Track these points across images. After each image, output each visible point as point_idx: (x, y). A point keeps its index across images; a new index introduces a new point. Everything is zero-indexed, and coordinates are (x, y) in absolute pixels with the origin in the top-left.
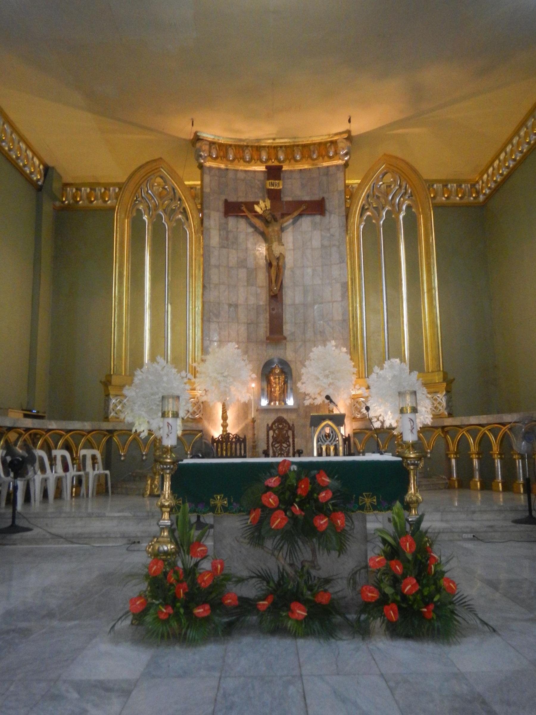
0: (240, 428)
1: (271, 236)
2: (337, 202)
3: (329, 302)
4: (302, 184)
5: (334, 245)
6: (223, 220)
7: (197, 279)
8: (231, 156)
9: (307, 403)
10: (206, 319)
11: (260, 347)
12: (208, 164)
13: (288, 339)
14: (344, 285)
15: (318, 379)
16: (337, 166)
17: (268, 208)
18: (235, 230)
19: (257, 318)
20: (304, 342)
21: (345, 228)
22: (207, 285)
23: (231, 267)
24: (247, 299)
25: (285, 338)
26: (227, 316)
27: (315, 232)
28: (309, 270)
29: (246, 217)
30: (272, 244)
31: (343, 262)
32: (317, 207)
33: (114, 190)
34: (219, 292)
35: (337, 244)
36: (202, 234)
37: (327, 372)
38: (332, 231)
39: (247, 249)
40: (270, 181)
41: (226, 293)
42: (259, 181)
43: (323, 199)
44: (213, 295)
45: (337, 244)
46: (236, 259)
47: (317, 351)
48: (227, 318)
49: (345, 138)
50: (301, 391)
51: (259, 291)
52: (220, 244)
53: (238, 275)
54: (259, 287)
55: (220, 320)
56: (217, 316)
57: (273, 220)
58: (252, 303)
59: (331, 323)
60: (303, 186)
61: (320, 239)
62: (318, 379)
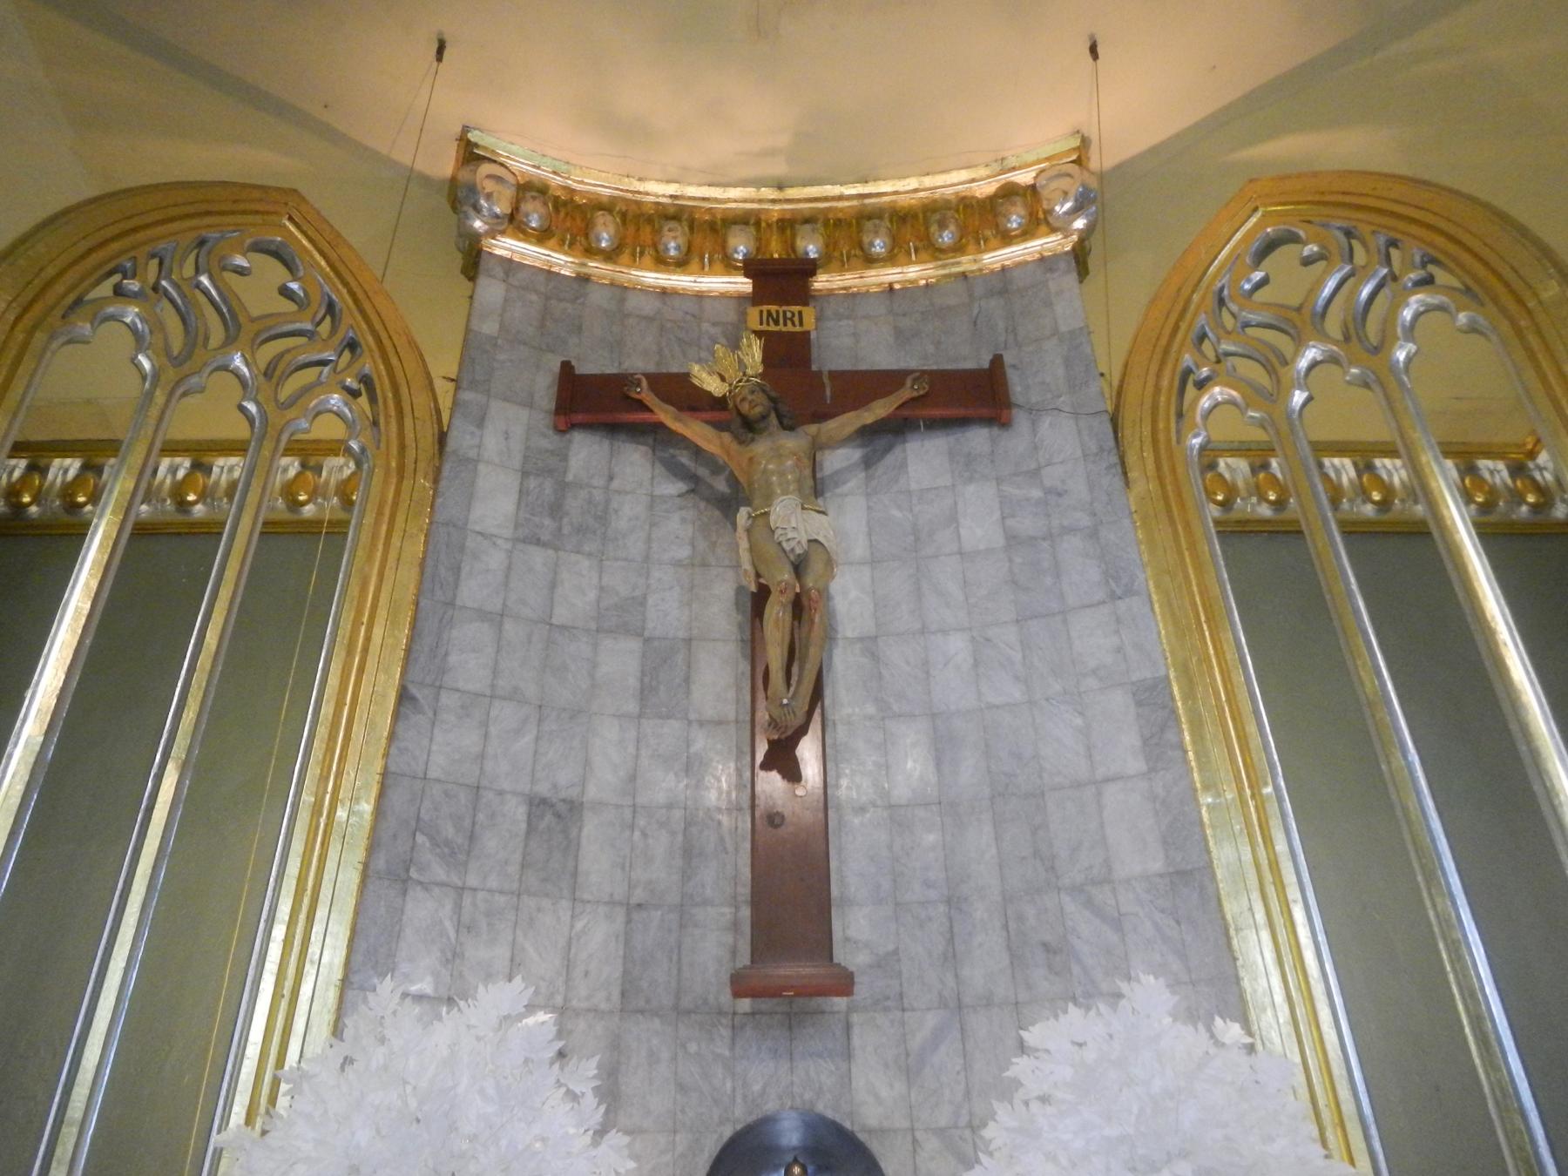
1: (765, 471)
2: (1061, 371)
3: (1078, 785)
4: (898, 332)
6: (549, 441)
10: (389, 871)
11: (693, 1047)
12: (506, 246)
13: (862, 990)
14: (1151, 696)
16: (1045, 263)
17: (749, 371)
18: (599, 482)
19: (686, 875)
20: (957, 1007)
21: (1114, 459)
23: (563, 628)
24: (633, 778)
25: (844, 984)
26: (518, 857)
27: (971, 488)
28: (957, 645)
29: (654, 434)
30: (769, 498)
31: (1129, 592)
32: (973, 397)
33: (173, 470)
35: (1085, 521)
36: (436, 481)
38: (1052, 476)
40: (765, 308)
41: (527, 739)
42: (714, 324)
43: (997, 361)
44: (446, 746)
45: (1085, 521)
46: (592, 595)
47: (1061, 1041)
48: (513, 869)
51: (700, 741)
52: (516, 527)
53: (595, 665)
54: (701, 724)
55: (472, 880)
56: (460, 853)
57: (773, 419)
58: (661, 798)
61: (997, 515)
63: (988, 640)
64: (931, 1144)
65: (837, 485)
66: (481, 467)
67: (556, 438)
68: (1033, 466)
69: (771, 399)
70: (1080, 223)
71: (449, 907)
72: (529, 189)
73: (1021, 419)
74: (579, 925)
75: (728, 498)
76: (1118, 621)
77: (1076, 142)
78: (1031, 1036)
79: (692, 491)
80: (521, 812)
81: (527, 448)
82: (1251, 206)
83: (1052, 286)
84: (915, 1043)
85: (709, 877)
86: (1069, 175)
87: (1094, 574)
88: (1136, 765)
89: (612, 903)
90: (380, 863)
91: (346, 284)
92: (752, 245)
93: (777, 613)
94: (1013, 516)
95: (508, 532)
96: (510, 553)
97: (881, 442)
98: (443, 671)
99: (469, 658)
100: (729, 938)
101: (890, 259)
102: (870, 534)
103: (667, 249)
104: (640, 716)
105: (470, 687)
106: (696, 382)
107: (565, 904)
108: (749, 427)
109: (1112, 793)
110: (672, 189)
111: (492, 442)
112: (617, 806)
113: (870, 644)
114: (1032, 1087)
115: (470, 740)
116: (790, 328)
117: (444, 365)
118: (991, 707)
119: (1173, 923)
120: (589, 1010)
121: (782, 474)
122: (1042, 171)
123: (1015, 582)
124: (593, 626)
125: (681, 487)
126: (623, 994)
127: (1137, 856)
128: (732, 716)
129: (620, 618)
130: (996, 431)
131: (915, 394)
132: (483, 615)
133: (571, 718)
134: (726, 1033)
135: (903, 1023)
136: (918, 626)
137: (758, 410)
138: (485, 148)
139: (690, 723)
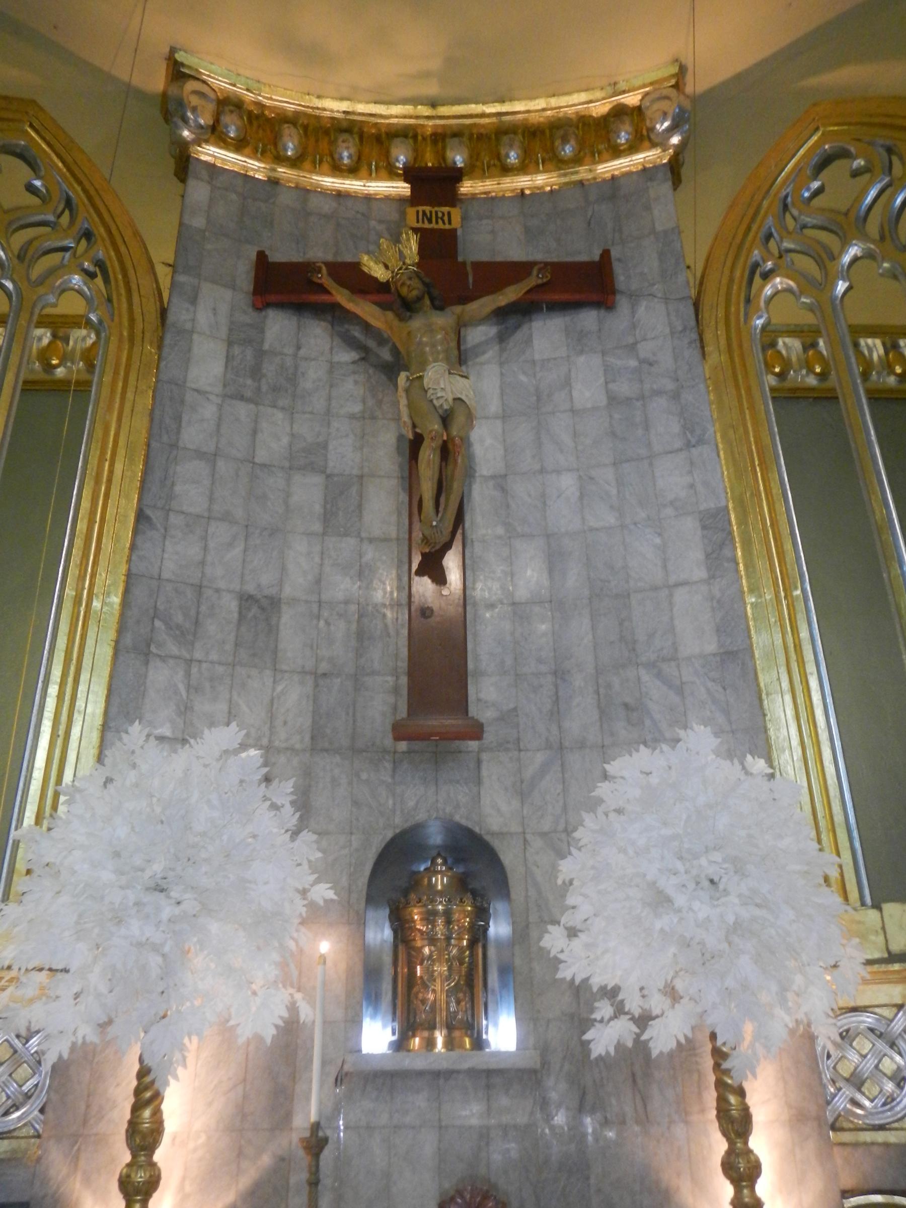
0: (245, 1182)
1: (420, 343)
2: (656, 264)
3: (655, 588)
4: (527, 230)
5: (658, 393)
6: (248, 317)
7: (114, 492)
8: (291, 145)
9: (606, 1038)
10: (135, 645)
11: (364, 776)
12: (210, 153)
13: (490, 736)
14: (714, 523)
15: (660, 900)
16: (647, 172)
17: (408, 261)
18: (289, 350)
19: (359, 652)
20: (560, 749)
21: (694, 336)
22: (155, 515)
23: (264, 466)
24: (318, 581)
25: (476, 731)
26: (232, 637)
27: (582, 359)
28: (568, 482)
29: (333, 313)
30: (423, 366)
31: (701, 441)
32: (585, 285)
34: (205, 548)
36: (160, 347)
37: (708, 865)
38: (645, 350)
39: (328, 412)
40: (421, 208)
41: (237, 551)
42: (380, 222)
43: (606, 254)
44: (175, 555)
45: (670, 386)
46: (285, 440)
47: (632, 771)
48: (229, 647)
49: (672, 86)
50: (565, 973)
51: (370, 553)
52: (225, 386)
53: (288, 495)
54: (371, 540)
55: (198, 655)
56: (189, 633)
57: (427, 302)
58: (340, 596)
59: (669, 669)
60: (531, 235)
61: (602, 380)
62: (660, 900)
63: (591, 478)
64: (537, 843)
65: (477, 356)
66: (195, 337)
67: (255, 314)
68: (631, 340)
69: (424, 283)
70: (675, 140)
71: (181, 673)
72: (228, 104)
73: (623, 303)
74: (279, 688)
75: (391, 365)
76: (692, 463)
77: (674, 70)
78: (611, 768)
79: (363, 359)
80: (234, 605)
81: (232, 323)
82: (812, 126)
83: (652, 193)
84: (528, 773)
85: (375, 655)
86: (667, 98)
87: (676, 428)
88: (701, 573)
89: (303, 672)
90: (128, 640)
91: (80, 183)
92: (410, 155)
93: (428, 455)
94: (614, 381)
95: (218, 389)
96: (220, 407)
97: (512, 321)
98: (171, 497)
99: (191, 489)
100: (391, 699)
101: (522, 169)
102: (502, 394)
103: (341, 158)
104: (324, 534)
105: (192, 510)
106: (366, 269)
107: (268, 672)
108: (407, 308)
109: (680, 595)
110: (344, 106)
111: (203, 317)
112: (306, 602)
113: (500, 481)
114: (611, 802)
115: (194, 551)
116: (441, 225)
117: (163, 252)
118: (591, 529)
119: (721, 690)
120: (287, 749)
121: (433, 346)
122: (646, 94)
123: (614, 434)
124: (287, 464)
125: (353, 355)
126: (312, 738)
127: (697, 639)
128: (394, 535)
129: (307, 458)
130: (603, 312)
131: (540, 282)
132: (200, 455)
133: (270, 535)
134: (389, 765)
135: (519, 760)
136: (537, 467)
137: (415, 293)
138: (189, 67)
139: (362, 540)
